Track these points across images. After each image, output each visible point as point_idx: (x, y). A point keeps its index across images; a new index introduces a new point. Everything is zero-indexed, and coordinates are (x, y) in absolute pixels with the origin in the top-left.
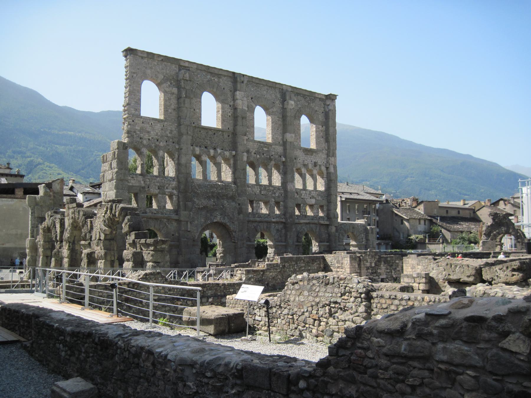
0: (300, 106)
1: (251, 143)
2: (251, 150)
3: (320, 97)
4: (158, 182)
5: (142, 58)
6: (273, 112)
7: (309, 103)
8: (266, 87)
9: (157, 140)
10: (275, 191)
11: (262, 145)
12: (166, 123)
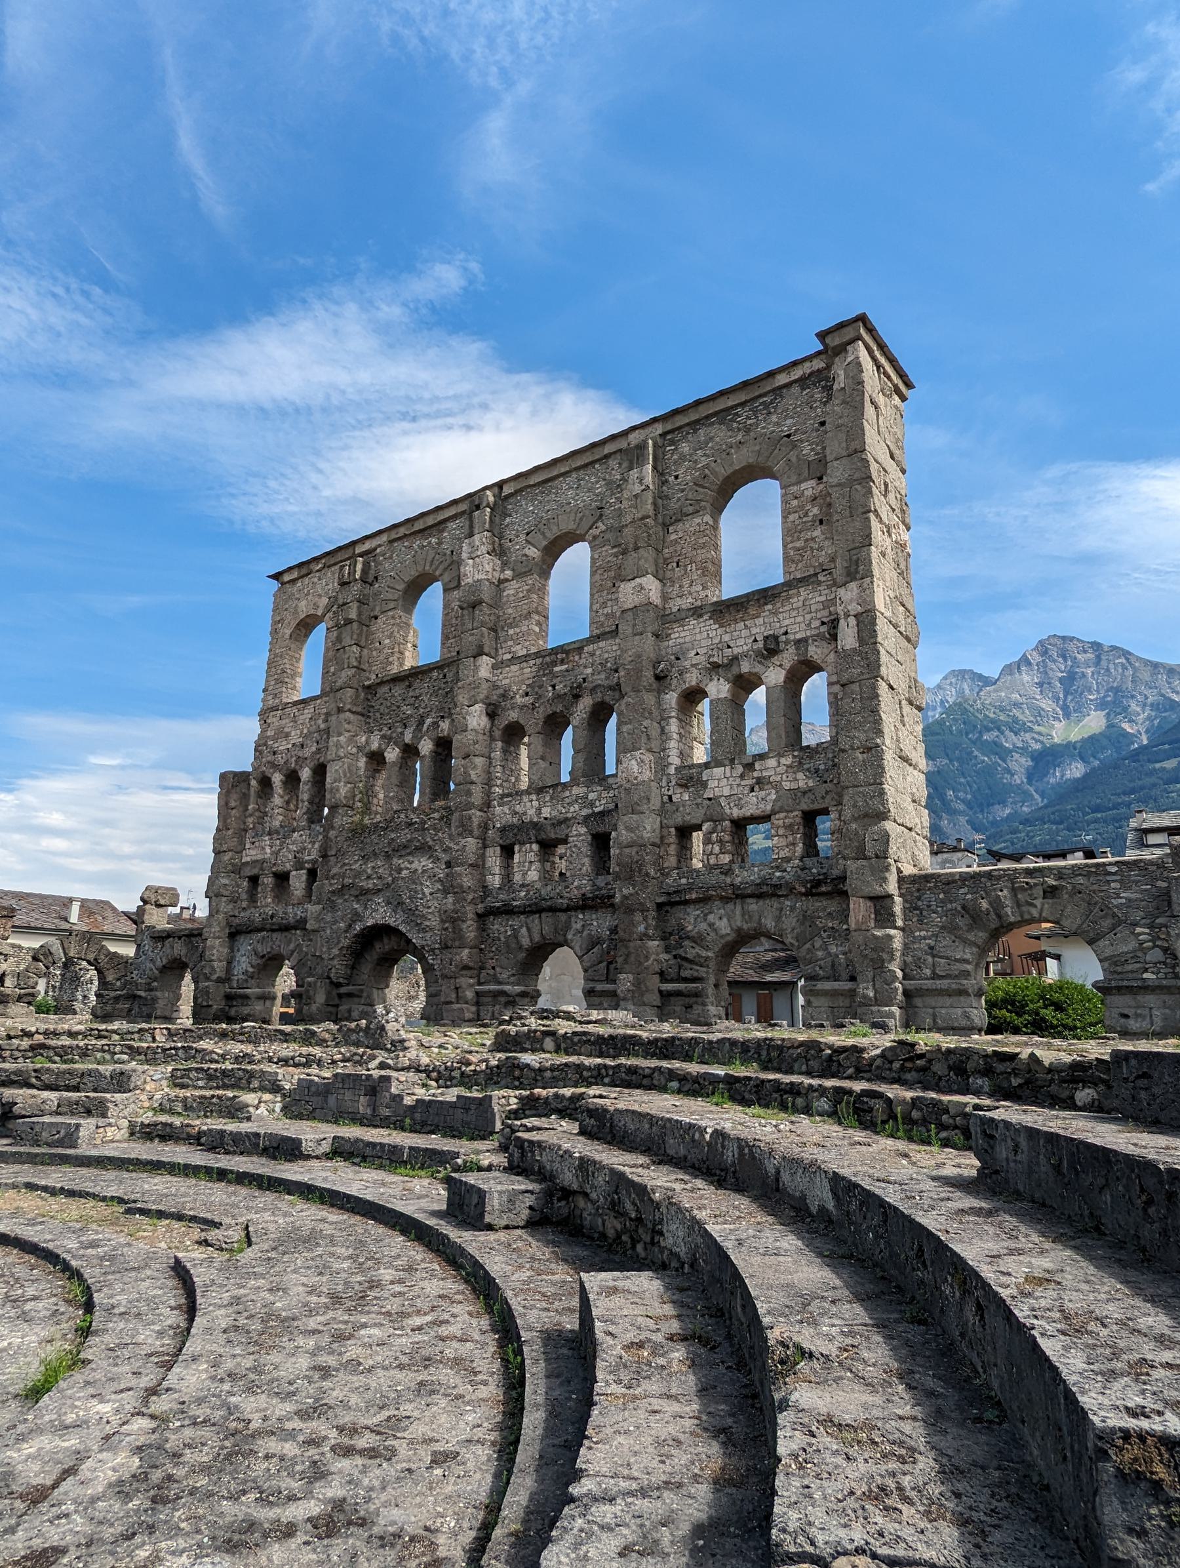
0: (704, 461)
3: (797, 374)
5: (293, 581)
6: (595, 537)
7: (748, 430)
8: (574, 475)
10: (592, 796)
11: (548, 659)
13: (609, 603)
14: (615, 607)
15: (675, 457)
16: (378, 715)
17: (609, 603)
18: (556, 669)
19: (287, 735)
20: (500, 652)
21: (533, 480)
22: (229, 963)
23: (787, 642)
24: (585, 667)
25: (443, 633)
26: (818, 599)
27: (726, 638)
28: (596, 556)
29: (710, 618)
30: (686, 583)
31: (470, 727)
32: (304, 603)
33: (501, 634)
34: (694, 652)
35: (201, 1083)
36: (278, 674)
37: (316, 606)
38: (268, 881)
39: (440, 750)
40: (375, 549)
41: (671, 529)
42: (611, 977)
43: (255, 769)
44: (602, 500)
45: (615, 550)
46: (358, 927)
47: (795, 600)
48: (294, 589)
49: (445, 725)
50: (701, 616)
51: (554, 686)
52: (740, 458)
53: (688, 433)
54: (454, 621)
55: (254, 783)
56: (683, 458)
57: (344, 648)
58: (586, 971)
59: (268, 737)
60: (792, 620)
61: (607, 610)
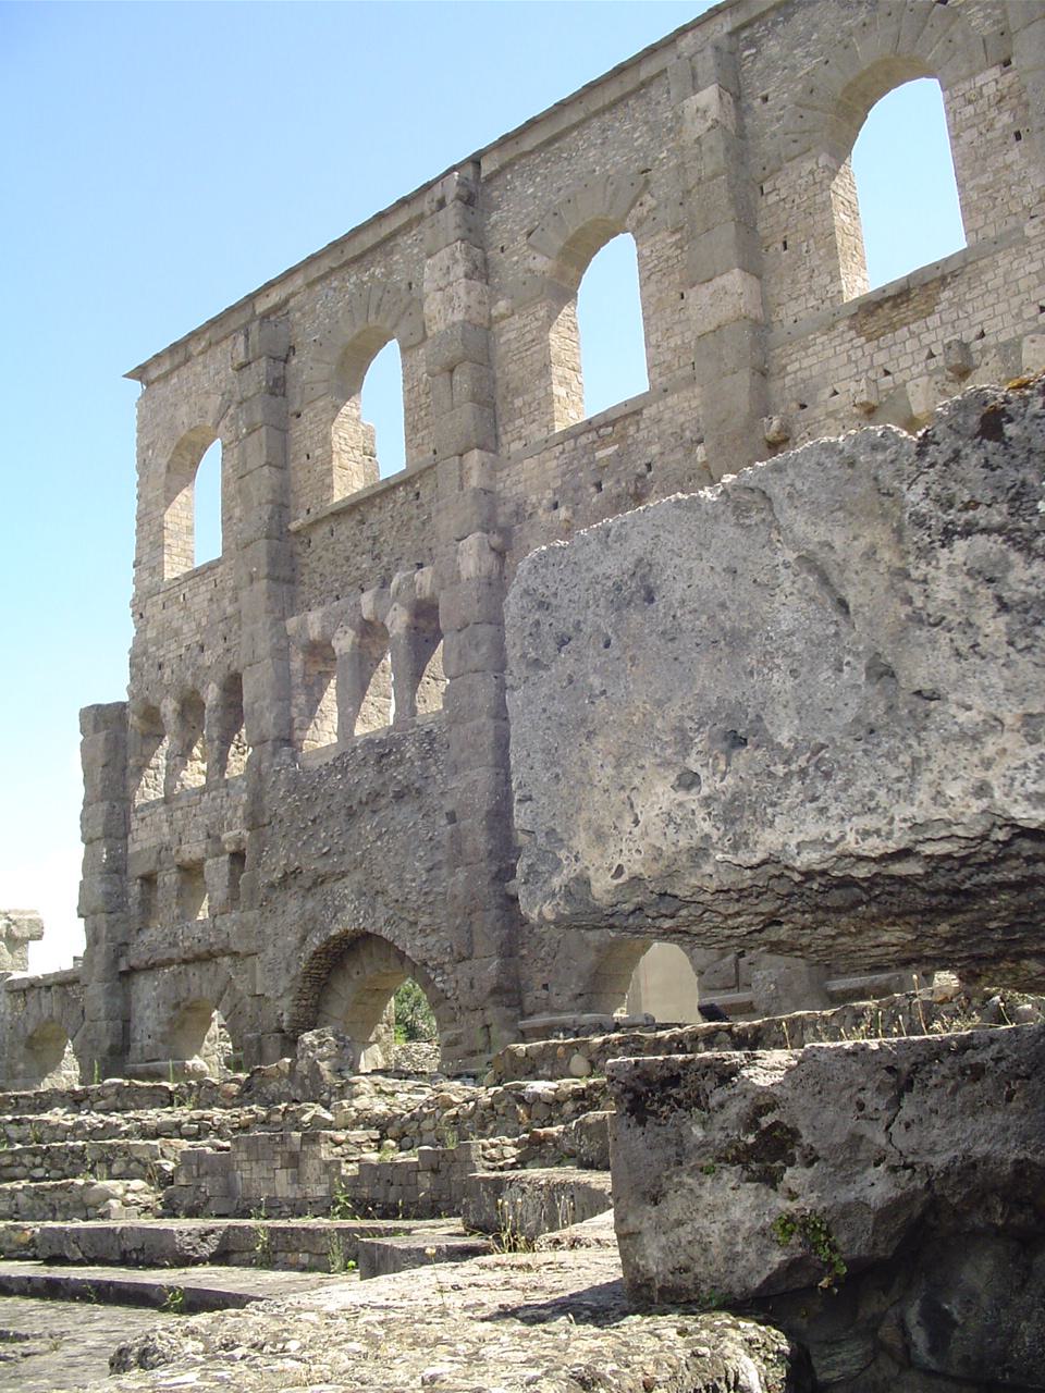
0: (808, 65)
1: (529, 463)
2: (533, 498)
4: (204, 812)
5: (165, 377)
6: (640, 222)
8: (596, 123)
9: (202, 649)
11: (583, 440)
12: (220, 569)
13: (678, 329)
14: (688, 334)
15: (759, 65)
16: (316, 576)
17: (678, 329)
18: (600, 454)
19: (177, 633)
20: (504, 439)
21: (528, 143)
22: (127, 1021)
23: (984, 352)
24: (649, 443)
25: (407, 423)
26: (1028, 268)
27: (881, 358)
28: (647, 252)
29: (850, 328)
30: (802, 275)
31: (464, 575)
32: (184, 409)
33: (500, 408)
34: (828, 391)
35: (39, 1172)
36: (151, 537)
37: (203, 414)
38: (169, 878)
39: (422, 623)
40: (287, 301)
41: (767, 187)
42: (743, 978)
43: (132, 696)
44: (646, 157)
45: (678, 236)
46: (316, 941)
47: (990, 275)
48: (161, 390)
49: (425, 579)
50: (833, 326)
51: (599, 486)
52: (868, 50)
53: (775, 24)
54: (423, 400)
55: (133, 720)
56: (771, 65)
57: (250, 472)
58: (700, 973)
59: (146, 641)
60: (989, 311)
61: (676, 341)
